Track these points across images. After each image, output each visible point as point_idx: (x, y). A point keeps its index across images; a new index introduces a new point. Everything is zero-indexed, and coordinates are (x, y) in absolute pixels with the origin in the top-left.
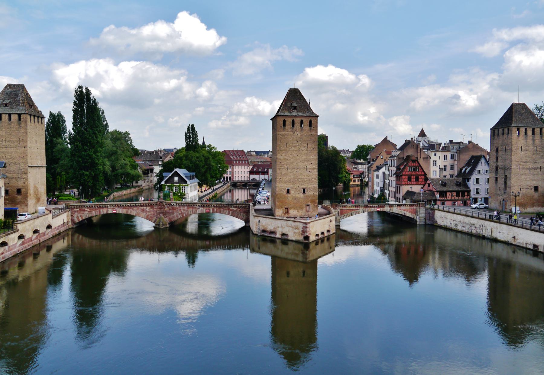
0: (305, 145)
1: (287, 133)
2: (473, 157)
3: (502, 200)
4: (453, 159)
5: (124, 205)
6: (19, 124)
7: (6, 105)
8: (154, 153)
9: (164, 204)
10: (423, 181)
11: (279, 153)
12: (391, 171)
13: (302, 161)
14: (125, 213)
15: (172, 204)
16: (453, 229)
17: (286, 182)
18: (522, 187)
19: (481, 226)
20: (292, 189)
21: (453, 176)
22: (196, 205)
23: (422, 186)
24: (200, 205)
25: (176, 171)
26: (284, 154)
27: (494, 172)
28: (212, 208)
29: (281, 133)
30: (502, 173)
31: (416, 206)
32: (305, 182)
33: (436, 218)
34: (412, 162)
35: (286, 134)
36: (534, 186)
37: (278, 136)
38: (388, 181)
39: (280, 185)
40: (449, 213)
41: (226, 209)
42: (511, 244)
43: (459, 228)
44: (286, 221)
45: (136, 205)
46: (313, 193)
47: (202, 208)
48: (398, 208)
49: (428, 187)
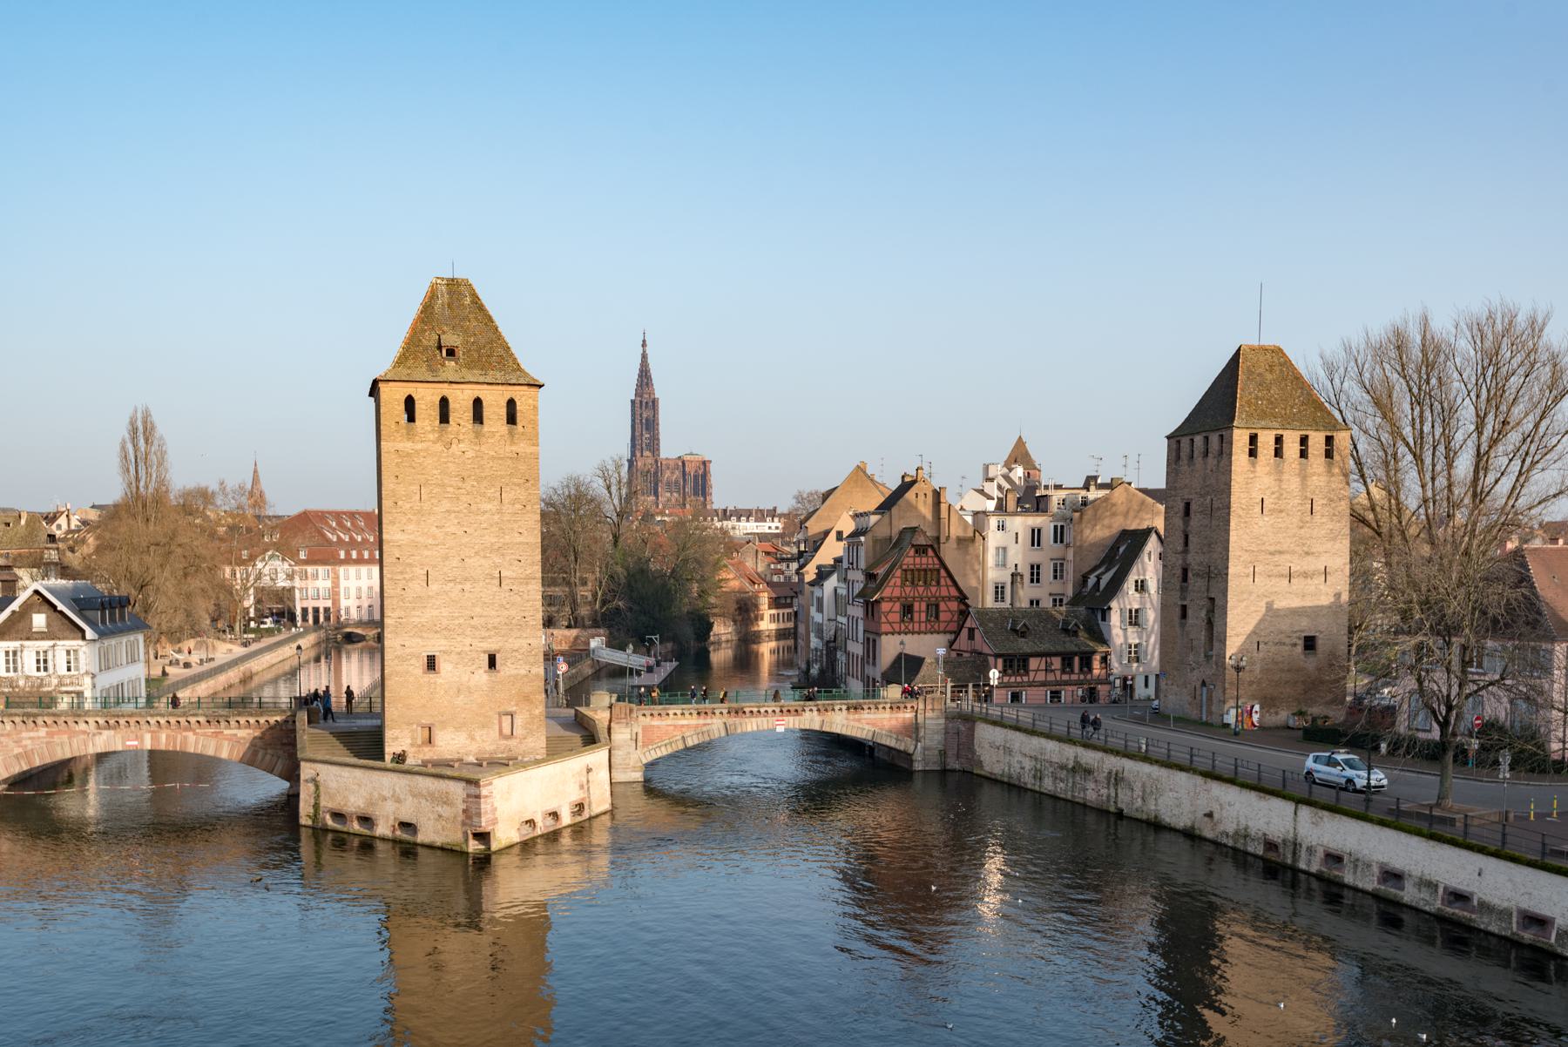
2: (1125, 534)
3: (1198, 684)
4: (1062, 541)
8: (23, 522)
10: (955, 618)
13: (482, 554)
16: (1029, 786)
18: (1261, 640)
19: (1113, 780)
20: (446, 657)
21: (1061, 600)
22: (87, 722)
23: (953, 636)
24: (101, 721)
26: (411, 527)
27: (1178, 587)
28: (150, 732)
30: (1199, 592)
31: (912, 707)
32: (495, 628)
33: (978, 750)
34: (916, 552)
36: (1304, 635)
40: (1018, 733)
41: (205, 735)
42: (1205, 839)
43: (1048, 785)
44: (409, 776)
46: (527, 668)
47: (112, 732)
48: (851, 717)
49: (969, 639)
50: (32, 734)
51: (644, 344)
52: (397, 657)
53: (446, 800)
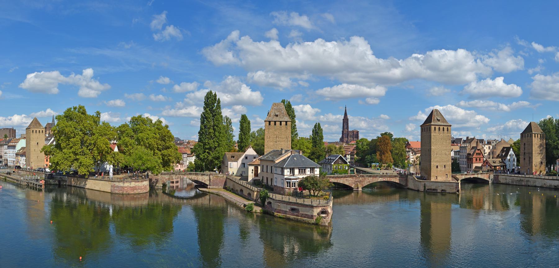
5: (336, 177)
6: (287, 128)
7: (277, 116)
9: (360, 176)
11: (433, 145)
12: (461, 155)
14: (337, 182)
17: (436, 162)
25: (341, 156)
26: (435, 146)
29: (434, 134)
37: (432, 136)
38: (459, 161)
50: (370, 178)
51: (346, 108)
52: (433, 166)
53: (452, 186)
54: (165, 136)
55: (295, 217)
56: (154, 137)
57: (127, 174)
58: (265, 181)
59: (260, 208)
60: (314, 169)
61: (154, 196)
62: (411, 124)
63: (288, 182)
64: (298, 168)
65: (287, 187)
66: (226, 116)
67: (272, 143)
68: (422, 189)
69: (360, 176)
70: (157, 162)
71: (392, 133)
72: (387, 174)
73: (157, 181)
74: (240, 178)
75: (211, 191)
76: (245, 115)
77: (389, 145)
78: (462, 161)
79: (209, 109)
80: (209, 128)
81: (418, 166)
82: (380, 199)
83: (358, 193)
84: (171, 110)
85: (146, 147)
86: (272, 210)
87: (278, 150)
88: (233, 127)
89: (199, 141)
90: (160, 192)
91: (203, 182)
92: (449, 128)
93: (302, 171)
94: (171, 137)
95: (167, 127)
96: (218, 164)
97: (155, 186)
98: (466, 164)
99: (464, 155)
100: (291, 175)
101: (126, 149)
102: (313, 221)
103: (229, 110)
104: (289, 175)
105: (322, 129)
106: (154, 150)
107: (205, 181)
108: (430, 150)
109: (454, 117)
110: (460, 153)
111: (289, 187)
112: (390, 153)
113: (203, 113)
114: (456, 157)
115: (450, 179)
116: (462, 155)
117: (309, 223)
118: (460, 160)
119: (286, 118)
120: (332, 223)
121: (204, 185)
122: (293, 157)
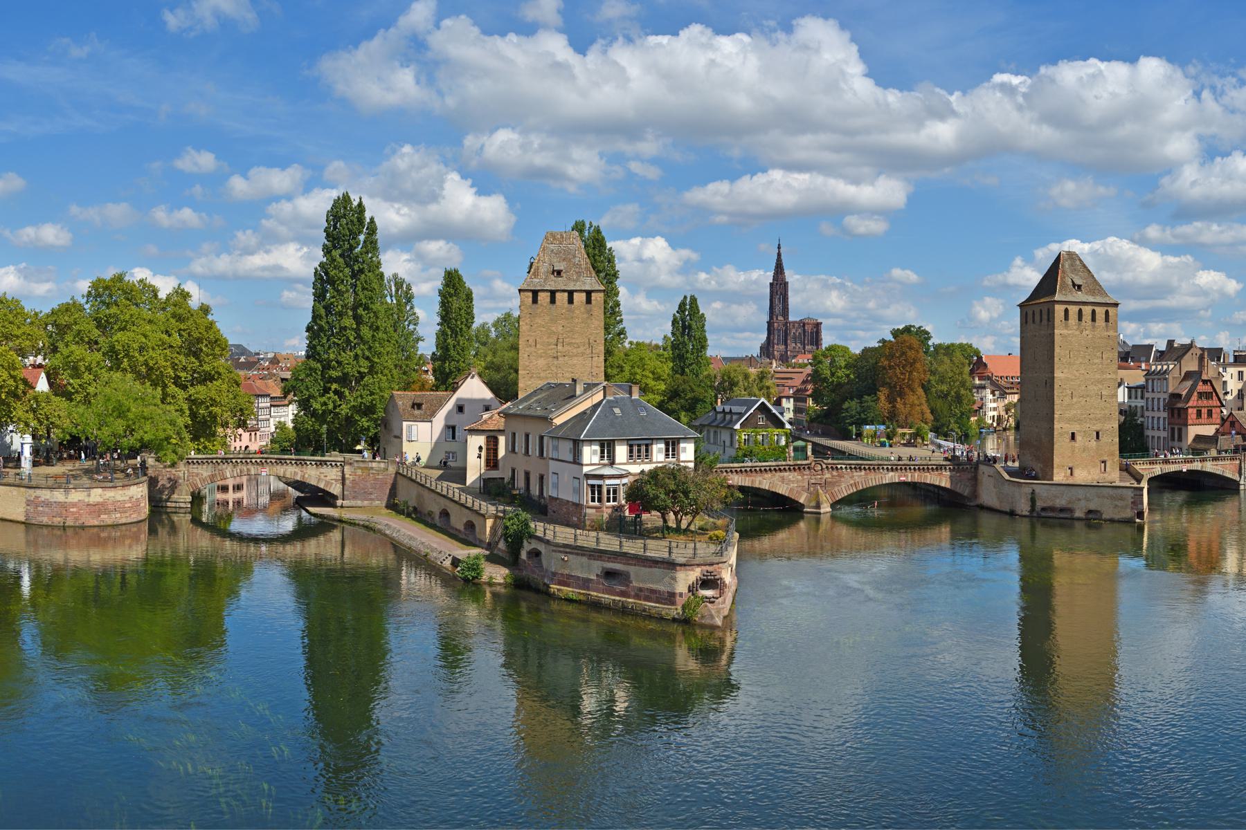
0: (1099, 354)
1: (1070, 332)
7: (559, 273)
9: (824, 466)
11: (1058, 368)
14: (750, 485)
15: (839, 466)
17: (1069, 421)
24: (890, 467)
25: (763, 403)
26: (1065, 371)
35: (1069, 334)
37: (1056, 337)
38: (1141, 419)
39: (1060, 425)
45: (770, 469)
50: (859, 474)
51: (779, 248)
54: (199, 340)
55: (618, 598)
56: (164, 343)
57: (77, 464)
58: (520, 483)
59: (505, 571)
60: (679, 443)
61: (163, 532)
62: (988, 300)
63: (593, 486)
64: (628, 440)
65: (591, 504)
66: (395, 276)
67: (541, 362)
68: (1023, 507)
69: (824, 466)
70: (172, 423)
71: (928, 329)
72: (910, 458)
73: (174, 484)
74: (441, 472)
75: (346, 515)
76: (456, 271)
77: (918, 365)
78: (1153, 418)
79: (339, 251)
80: (341, 314)
81: (1011, 435)
82: (888, 539)
83: (818, 521)
84: (218, 256)
85: (139, 377)
86: (543, 577)
87: (560, 384)
88: (417, 310)
89: (308, 357)
90: (183, 520)
91: (322, 486)
92: (1111, 310)
93: (639, 451)
94: (218, 342)
95: (205, 310)
96: (368, 429)
97: (167, 500)
98: (1164, 428)
99: (1159, 399)
100: (605, 465)
101: (75, 382)
102: (675, 611)
103: (405, 256)
104: (599, 464)
105: (703, 314)
106: (165, 387)
107: (327, 483)
108: (1050, 383)
109: (1128, 277)
110: (1148, 392)
111: (596, 504)
112: (920, 391)
113: (322, 265)
114: (1133, 405)
115: (1114, 476)
116: (1153, 399)
117: (661, 619)
118: (1147, 414)
119: (588, 280)
120: (735, 618)
121: (326, 498)
122: (611, 405)
